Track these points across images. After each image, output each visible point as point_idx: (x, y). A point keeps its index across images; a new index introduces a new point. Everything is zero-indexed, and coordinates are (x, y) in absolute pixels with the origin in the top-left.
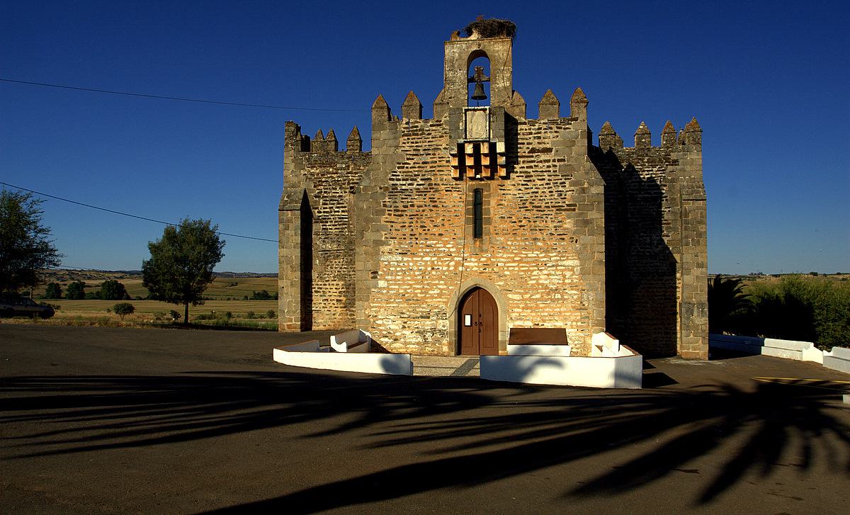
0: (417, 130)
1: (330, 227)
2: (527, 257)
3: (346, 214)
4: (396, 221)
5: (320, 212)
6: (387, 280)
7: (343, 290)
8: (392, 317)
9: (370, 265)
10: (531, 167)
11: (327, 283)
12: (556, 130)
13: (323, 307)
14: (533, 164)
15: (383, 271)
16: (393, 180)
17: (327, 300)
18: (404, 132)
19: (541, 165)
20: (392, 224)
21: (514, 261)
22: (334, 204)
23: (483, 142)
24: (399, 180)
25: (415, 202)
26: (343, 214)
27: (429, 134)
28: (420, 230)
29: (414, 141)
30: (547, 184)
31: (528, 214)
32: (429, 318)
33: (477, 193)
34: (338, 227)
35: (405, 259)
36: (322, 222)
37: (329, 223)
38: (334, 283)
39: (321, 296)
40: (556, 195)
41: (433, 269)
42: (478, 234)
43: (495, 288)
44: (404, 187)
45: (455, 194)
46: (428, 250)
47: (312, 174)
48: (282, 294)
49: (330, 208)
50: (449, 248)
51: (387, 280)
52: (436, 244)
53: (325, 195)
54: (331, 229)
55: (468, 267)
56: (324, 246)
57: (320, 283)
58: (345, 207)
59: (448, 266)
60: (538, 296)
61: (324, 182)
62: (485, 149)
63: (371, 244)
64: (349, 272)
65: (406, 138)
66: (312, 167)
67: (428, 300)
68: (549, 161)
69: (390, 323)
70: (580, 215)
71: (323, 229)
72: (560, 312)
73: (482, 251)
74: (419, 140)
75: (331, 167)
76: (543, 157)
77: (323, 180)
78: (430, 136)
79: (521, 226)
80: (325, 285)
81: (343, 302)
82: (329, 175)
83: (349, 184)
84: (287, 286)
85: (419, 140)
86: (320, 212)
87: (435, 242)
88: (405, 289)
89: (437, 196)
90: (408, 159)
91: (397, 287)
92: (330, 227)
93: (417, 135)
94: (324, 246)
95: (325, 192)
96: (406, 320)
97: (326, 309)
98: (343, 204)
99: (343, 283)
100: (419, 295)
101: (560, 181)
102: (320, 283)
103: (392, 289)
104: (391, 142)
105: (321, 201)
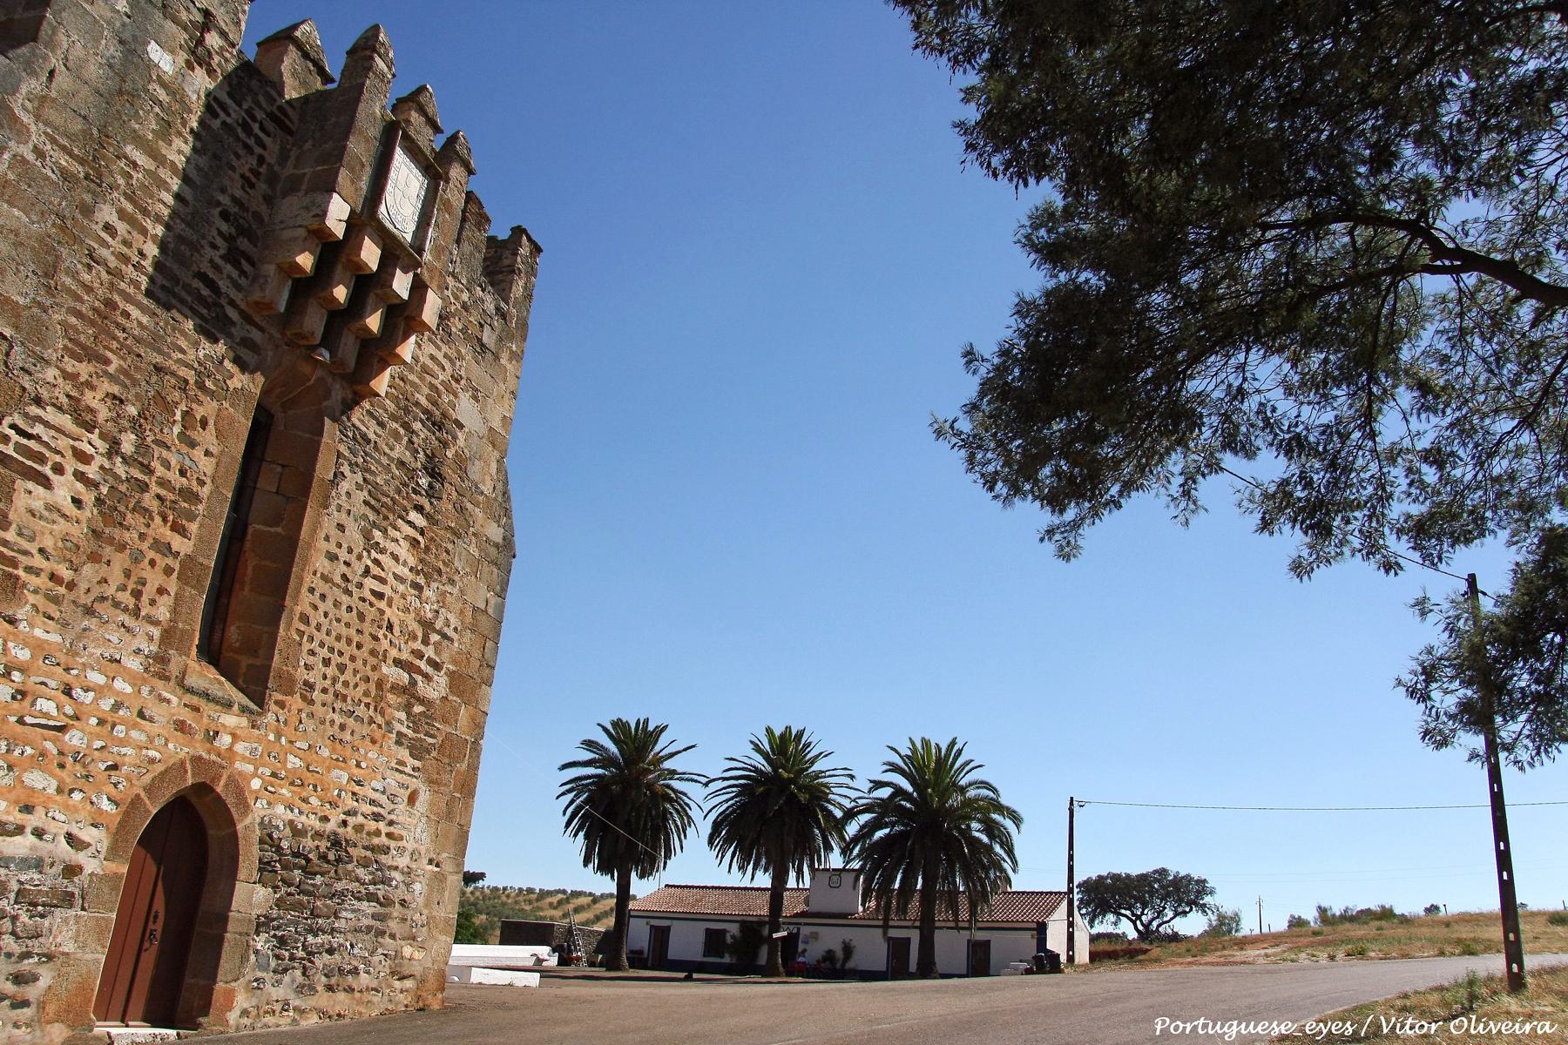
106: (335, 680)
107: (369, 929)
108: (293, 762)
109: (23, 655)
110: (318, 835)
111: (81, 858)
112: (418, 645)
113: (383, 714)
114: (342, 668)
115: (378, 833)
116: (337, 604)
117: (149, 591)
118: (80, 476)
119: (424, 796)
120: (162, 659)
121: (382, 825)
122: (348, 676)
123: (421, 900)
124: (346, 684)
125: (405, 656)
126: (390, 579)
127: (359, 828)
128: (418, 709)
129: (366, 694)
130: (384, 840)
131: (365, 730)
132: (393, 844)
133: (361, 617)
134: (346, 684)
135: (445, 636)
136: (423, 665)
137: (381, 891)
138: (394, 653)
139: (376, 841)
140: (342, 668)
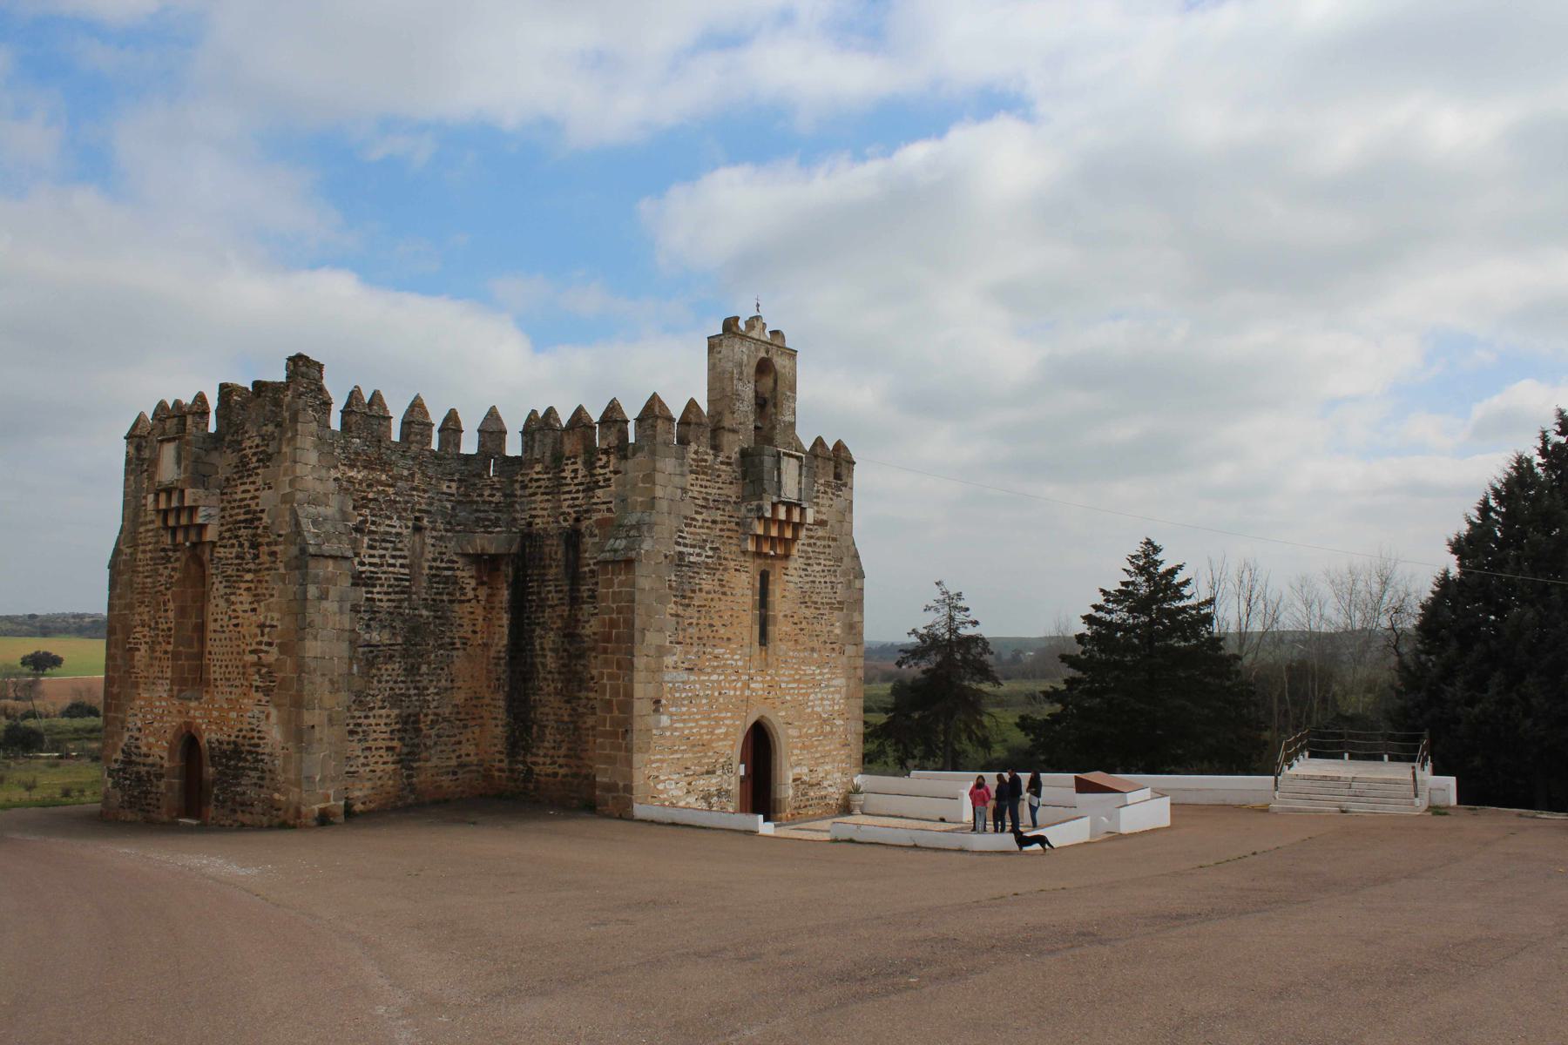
5: (362, 564)
6: (672, 715)
8: (675, 777)
9: (651, 691)
13: (364, 765)
16: (678, 544)
21: (795, 681)
24: (685, 545)
25: (706, 587)
28: (708, 631)
31: (808, 613)
32: (714, 772)
33: (764, 577)
34: (393, 597)
36: (366, 585)
38: (383, 712)
43: (777, 720)
44: (692, 559)
45: (744, 576)
47: (350, 480)
49: (382, 556)
51: (672, 715)
55: (753, 690)
56: (367, 636)
57: (357, 714)
58: (405, 557)
60: (812, 731)
63: (652, 652)
66: (352, 466)
68: (823, 538)
75: (383, 471)
76: (820, 533)
77: (371, 496)
80: (367, 717)
83: (413, 510)
86: (362, 564)
89: (726, 577)
93: (705, 473)
94: (367, 636)
95: (373, 523)
99: (397, 711)
102: (357, 714)
104: (677, 480)
105: (366, 540)
108: (215, 714)
119: (274, 713)
121: (255, 734)
125: (254, 647)
128: (264, 670)
131: (239, 691)
136: (263, 647)
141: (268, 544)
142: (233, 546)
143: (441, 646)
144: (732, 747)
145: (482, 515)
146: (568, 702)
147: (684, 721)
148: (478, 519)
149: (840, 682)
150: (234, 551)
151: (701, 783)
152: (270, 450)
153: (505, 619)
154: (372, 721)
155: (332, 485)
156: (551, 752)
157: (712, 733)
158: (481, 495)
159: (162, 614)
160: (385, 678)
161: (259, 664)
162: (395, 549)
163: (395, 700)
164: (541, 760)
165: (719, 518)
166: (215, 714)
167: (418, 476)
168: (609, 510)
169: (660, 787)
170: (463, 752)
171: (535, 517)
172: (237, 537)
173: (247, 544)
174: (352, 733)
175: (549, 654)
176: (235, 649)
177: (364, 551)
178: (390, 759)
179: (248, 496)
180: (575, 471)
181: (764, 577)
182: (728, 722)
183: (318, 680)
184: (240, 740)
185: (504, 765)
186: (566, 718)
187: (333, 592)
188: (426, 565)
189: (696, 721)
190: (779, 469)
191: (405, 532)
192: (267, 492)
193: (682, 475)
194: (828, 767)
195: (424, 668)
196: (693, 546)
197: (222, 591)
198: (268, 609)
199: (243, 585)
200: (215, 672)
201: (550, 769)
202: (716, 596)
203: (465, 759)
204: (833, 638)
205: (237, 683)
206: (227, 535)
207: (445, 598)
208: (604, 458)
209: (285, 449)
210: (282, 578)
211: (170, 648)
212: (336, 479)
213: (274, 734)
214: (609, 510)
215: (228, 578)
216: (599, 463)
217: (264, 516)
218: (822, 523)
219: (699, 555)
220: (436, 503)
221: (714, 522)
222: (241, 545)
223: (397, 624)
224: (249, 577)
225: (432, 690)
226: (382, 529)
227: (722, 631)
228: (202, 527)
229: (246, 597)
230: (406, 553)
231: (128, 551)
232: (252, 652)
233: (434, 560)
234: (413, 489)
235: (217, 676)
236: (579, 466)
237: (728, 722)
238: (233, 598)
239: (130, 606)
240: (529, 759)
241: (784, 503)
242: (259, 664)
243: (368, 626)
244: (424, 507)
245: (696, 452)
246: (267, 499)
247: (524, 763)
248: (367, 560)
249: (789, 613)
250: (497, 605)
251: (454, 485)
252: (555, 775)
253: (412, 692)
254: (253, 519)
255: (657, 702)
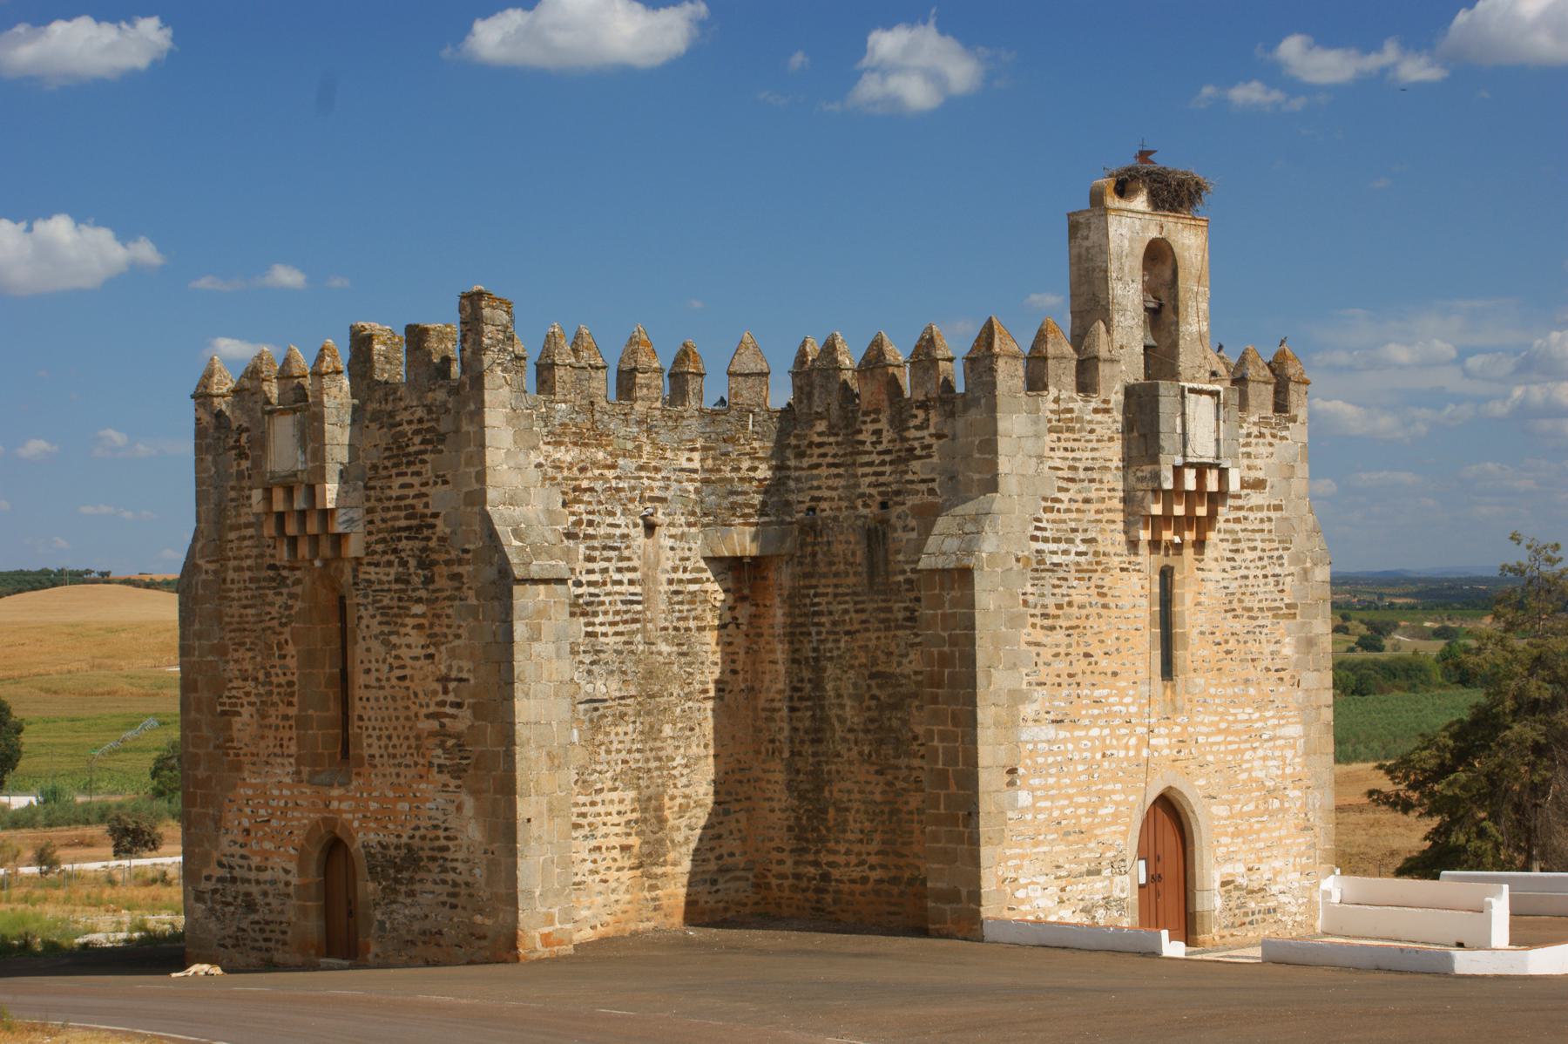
0: (1071, 420)
1: (604, 629)
2: (1236, 721)
3: (638, 589)
4: (1044, 640)
5: (578, 584)
7: (635, 815)
8: (1042, 879)
9: (1004, 758)
10: (1237, 520)
11: (598, 798)
12: (1269, 439)
14: (1241, 514)
15: (1026, 767)
16: (1034, 538)
17: (599, 848)
18: (1050, 421)
19: (1251, 516)
20: (1038, 649)
21: (1220, 732)
22: (609, 560)
23: (1211, 466)
24: (1046, 540)
26: (632, 589)
27: (1092, 431)
28: (1084, 663)
29: (1069, 445)
30: (1261, 559)
31: (1237, 626)
32: (1098, 872)
33: (1166, 575)
34: (621, 628)
35: (1062, 734)
36: (584, 614)
37: (600, 619)
38: (615, 795)
39: (586, 837)
40: (1271, 580)
41: (1104, 755)
42: (1168, 670)
43: (1193, 792)
44: (1056, 559)
45: (1135, 577)
46: (1096, 712)
48: (527, 843)
49: (605, 570)
50: (1127, 705)
51: (1033, 790)
52: (1107, 697)
53: (590, 531)
54: (605, 635)
56: (589, 688)
57: (582, 799)
58: (634, 569)
59: (1127, 748)
61: (586, 490)
62: (1212, 484)
63: (1004, 699)
64: (647, 760)
65: (1055, 436)
66: (558, 444)
67: (1097, 832)
68: (1260, 508)
69: (1039, 893)
70: (1304, 624)
71: (588, 634)
72: (1280, 839)
73: (1175, 710)
74: (1076, 445)
75: (599, 446)
77: (585, 484)
78: (1093, 437)
79: (1228, 652)
80: (593, 804)
81: (636, 850)
82: (597, 472)
84: (541, 813)
85: (1076, 445)
87: (1105, 692)
88: (1062, 808)
90: (1060, 489)
91: (1048, 804)
92: (604, 629)
94: (589, 688)
95: (590, 523)
96: (1063, 883)
97: (598, 878)
98: (629, 559)
99: (632, 794)
100: (1083, 820)
101: (1276, 554)
102: (582, 799)
103: (1041, 810)
104: (1029, 445)
105: (582, 548)
106: (386, 747)
107: (444, 904)
108: (373, 806)
109: (250, 792)
110: (398, 847)
111: (289, 877)
112: (441, 697)
113: (423, 756)
114: (390, 738)
115: (437, 838)
116: (377, 699)
117: (285, 743)
118: (250, 704)
119: (469, 803)
120: (298, 773)
122: (395, 740)
123: (482, 881)
124: (394, 746)
125: (433, 709)
126: (409, 662)
127: (423, 838)
128: (450, 742)
129: (409, 747)
130: (443, 842)
131: (413, 771)
132: (451, 844)
133: (394, 699)
134: (394, 746)
135: (461, 680)
136: (448, 710)
137: (451, 876)
138: (424, 711)
139: (437, 844)
140: (390, 738)
141: (448, 563)
142: (390, 564)
143: (688, 697)
144: (1124, 834)
145: (740, 499)
146: (880, 772)
147: (1052, 798)
148: (733, 507)
149: (1295, 730)
150: (392, 571)
151: (1078, 889)
152: (442, 428)
153: (780, 652)
154: (600, 808)
155: (535, 475)
156: (856, 848)
157: (1093, 814)
158: (738, 469)
159: (277, 661)
160: (615, 746)
161: (443, 733)
162: (621, 559)
163: (631, 777)
164: (841, 859)
165: (1093, 495)
166: (373, 806)
167: (647, 448)
168: (931, 492)
169: (1021, 894)
170: (724, 851)
171: (819, 499)
172: (395, 551)
173: (412, 563)
174: (577, 826)
175: (848, 703)
176: (402, 714)
177: (581, 565)
178: (627, 863)
179: (412, 492)
180: (878, 432)
181: (1166, 575)
182: (1116, 797)
183: (533, 754)
184: (417, 842)
185: (788, 868)
186: (878, 797)
187: (546, 626)
188: (664, 578)
189: (1069, 797)
190: (1183, 414)
191: (633, 532)
192: (441, 488)
193: (1037, 436)
194: (1278, 864)
195: (667, 730)
196: (1057, 540)
197: (376, 629)
198: (452, 654)
199: (410, 621)
200: (369, 745)
201: (856, 874)
202: (1093, 611)
203: (728, 861)
204: (1279, 664)
205: (408, 760)
206: (380, 548)
207: (692, 624)
208: (921, 414)
209: (466, 427)
210: (473, 612)
211: (293, 711)
212: (539, 465)
213: (473, 833)
214: (931, 492)
215: (384, 611)
216: (917, 422)
217: (439, 522)
218: (1259, 485)
219: (1066, 552)
220: (674, 485)
221: (1087, 501)
222: (404, 563)
223: (629, 666)
224: (418, 609)
225: (679, 761)
226: (602, 531)
227: (1104, 663)
228: (339, 540)
229: (416, 638)
230: (635, 563)
231: (211, 567)
232: (428, 716)
233: (675, 569)
234: (641, 468)
235: (375, 751)
236: (884, 424)
237: (1116, 797)
238: (394, 639)
239: (221, 651)
240: (824, 858)
241: (1191, 465)
242: (443, 733)
243: (589, 672)
244: (657, 493)
245: (1057, 400)
246: (440, 498)
247: (816, 864)
248: (584, 578)
249: (1207, 628)
250: (766, 630)
251: (696, 456)
252: (865, 880)
253: (653, 764)
254: (421, 525)
255: (1012, 771)
